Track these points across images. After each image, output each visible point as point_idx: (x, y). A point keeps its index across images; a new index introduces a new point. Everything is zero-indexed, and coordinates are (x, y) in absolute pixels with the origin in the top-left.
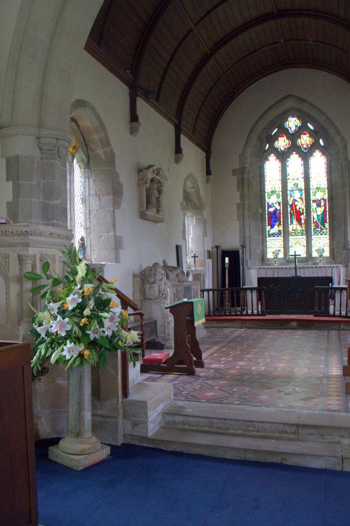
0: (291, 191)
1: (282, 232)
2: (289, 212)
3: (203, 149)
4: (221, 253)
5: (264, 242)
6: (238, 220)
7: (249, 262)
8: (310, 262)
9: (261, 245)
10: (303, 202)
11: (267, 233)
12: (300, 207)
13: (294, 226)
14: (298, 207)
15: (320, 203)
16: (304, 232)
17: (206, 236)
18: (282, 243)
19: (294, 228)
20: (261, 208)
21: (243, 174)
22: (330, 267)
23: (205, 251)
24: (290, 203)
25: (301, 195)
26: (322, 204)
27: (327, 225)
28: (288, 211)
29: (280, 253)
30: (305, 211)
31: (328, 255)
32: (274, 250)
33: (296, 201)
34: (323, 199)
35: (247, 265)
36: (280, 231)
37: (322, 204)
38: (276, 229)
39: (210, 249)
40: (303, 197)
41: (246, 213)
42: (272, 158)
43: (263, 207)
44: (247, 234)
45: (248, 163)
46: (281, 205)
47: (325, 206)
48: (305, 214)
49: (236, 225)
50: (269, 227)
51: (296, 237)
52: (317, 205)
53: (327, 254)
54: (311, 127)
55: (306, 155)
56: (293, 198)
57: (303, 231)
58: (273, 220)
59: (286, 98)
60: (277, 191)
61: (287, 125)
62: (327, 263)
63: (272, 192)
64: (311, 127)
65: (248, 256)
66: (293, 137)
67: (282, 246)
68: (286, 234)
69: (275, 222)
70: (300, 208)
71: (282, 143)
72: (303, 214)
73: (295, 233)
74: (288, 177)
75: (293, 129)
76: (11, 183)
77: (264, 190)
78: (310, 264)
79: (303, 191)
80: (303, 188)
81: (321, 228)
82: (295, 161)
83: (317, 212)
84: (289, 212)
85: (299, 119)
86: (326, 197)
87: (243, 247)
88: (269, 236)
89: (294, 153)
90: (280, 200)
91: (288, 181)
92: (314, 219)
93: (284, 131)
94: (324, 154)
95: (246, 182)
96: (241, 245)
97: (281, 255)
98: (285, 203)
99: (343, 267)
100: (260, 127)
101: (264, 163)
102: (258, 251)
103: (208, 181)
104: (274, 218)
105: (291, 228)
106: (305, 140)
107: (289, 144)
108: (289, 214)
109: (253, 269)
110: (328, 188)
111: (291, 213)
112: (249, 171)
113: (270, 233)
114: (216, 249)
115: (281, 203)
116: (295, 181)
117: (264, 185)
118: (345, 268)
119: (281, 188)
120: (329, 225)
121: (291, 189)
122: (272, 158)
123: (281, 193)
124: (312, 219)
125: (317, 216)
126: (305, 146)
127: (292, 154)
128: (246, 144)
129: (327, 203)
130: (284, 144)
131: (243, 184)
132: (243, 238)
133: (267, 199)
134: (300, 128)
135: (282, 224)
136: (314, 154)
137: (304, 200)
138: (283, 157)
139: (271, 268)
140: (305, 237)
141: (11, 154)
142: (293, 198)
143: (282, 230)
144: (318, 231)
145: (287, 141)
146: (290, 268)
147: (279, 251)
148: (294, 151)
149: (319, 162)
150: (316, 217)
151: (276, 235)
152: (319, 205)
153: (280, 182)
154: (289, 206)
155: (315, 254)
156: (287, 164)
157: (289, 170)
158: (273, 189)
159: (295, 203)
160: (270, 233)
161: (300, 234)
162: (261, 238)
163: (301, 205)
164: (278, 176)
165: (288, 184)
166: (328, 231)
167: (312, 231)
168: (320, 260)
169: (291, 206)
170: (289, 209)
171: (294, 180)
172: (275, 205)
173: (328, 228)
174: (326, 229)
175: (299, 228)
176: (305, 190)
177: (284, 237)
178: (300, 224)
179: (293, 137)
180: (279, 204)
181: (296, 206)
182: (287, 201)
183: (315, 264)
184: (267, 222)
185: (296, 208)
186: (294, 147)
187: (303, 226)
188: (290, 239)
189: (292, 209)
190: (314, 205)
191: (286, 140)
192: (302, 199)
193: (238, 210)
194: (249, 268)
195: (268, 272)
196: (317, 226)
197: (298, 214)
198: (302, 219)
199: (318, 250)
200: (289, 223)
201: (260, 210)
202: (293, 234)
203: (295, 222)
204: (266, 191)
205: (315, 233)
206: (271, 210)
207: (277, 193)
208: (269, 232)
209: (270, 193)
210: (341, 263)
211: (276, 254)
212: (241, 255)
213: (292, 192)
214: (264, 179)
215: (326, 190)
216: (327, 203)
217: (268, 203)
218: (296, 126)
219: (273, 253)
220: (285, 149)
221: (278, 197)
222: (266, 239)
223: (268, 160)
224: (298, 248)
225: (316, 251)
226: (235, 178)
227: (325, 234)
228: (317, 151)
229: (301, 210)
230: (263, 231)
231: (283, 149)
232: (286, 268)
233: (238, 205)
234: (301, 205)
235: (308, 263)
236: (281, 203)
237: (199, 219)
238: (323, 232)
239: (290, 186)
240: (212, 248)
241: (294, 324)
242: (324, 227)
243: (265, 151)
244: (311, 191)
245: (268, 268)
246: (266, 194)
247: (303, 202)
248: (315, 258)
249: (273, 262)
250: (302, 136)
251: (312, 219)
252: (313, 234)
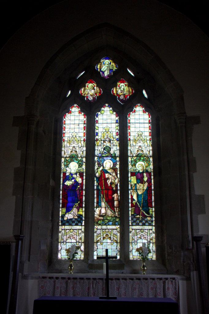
0: (99, 157)
1: (83, 219)
2: (95, 187)
6: (14, 194)
7: (26, 266)
8: (127, 269)
9: (49, 239)
10: (117, 175)
11: (60, 219)
13: (101, 210)
14: (109, 182)
15: (143, 177)
16: (117, 220)
22: (161, 279)
25: (115, 164)
26: (146, 179)
27: (152, 210)
28: (94, 186)
29: (79, 251)
30: (119, 188)
31: (154, 258)
32: (69, 246)
33: (108, 172)
34: (147, 172)
35: (22, 270)
36: (80, 216)
37: (146, 179)
40: (118, 166)
42: (75, 110)
44: (28, 217)
46: (84, 177)
47: (149, 181)
48: (119, 192)
50: (64, 210)
51: (104, 227)
52: (137, 179)
53: (152, 256)
55: (123, 110)
56: (101, 168)
57: (116, 217)
58: (70, 199)
60: (79, 156)
61: (98, 67)
62: (154, 272)
65: (25, 255)
66: (107, 84)
67: (83, 240)
68: (89, 222)
69: (74, 202)
70: (111, 183)
71: (90, 90)
72: (116, 192)
73: (103, 220)
75: (106, 74)
77: (61, 154)
78: (126, 273)
79: (118, 159)
80: (118, 153)
81: (143, 215)
83: (137, 191)
84: (95, 187)
85: (114, 62)
87: (18, 238)
88: (64, 224)
89: (107, 105)
91: (96, 142)
92: (133, 199)
96: (15, 236)
97: (80, 256)
98: (90, 174)
99: (182, 279)
101: (65, 116)
102: (44, 247)
104: (72, 196)
105: (97, 211)
106: (122, 89)
107: (100, 93)
108: (95, 192)
109: (32, 278)
110: (153, 156)
111: (98, 190)
113: (65, 219)
117: (61, 147)
118: (185, 282)
119: (85, 152)
120: (155, 211)
121: (100, 155)
122: (75, 110)
123: (84, 160)
124: (130, 201)
125: (138, 195)
126: (122, 97)
129: (152, 177)
132: (20, 224)
133: (63, 166)
134: (116, 73)
135: (84, 205)
138: (91, 110)
139: (63, 278)
142: (101, 168)
143: (84, 215)
144: (138, 219)
146: (94, 279)
147: (78, 248)
149: (140, 121)
150: (135, 197)
151: (74, 222)
152: (140, 180)
155: (134, 255)
158: (74, 153)
160: (65, 219)
161: (111, 223)
162: (51, 226)
163: (113, 179)
164: (81, 133)
166: (154, 219)
167: (130, 219)
168: (144, 266)
169: (99, 179)
170: (96, 183)
172: (75, 176)
173: (154, 215)
174: (151, 217)
175: (109, 212)
176: (120, 156)
179: (107, 84)
180: (81, 175)
181: (106, 179)
183: (135, 272)
184: (61, 201)
185: (106, 184)
186: (107, 98)
187: (117, 210)
188: (95, 230)
189: (100, 184)
190: (133, 180)
194: (25, 277)
195: (58, 285)
196: (137, 211)
197: (107, 192)
198: (116, 198)
199: (141, 248)
200: (95, 204)
201: (52, 183)
202: (99, 222)
205: (135, 222)
206: (68, 183)
207: (80, 159)
208: (63, 216)
209: (68, 159)
210: (177, 272)
211: (72, 252)
212: (13, 253)
213: (101, 159)
215: (151, 159)
216: (152, 177)
217: (65, 174)
218: (111, 70)
219: (68, 251)
220: (94, 98)
221: (80, 166)
222: (58, 229)
223: (70, 112)
224: (106, 246)
225: (138, 250)
227: (150, 225)
229: (113, 186)
231: (91, 98)
232: (88, 279)
234: (113, 179)
235: (124, 271)
238: (147, 221)
239: (98, 150)
242: (148, 213)
243: (65, 98)
244: (130, 159)
245: (57, 278)
246: (63, 160)
247: (117, 175)
248: (134, 261)
249: (67, 266)
250: (118, 83)
251: (130, 201)
252: (130, 224)
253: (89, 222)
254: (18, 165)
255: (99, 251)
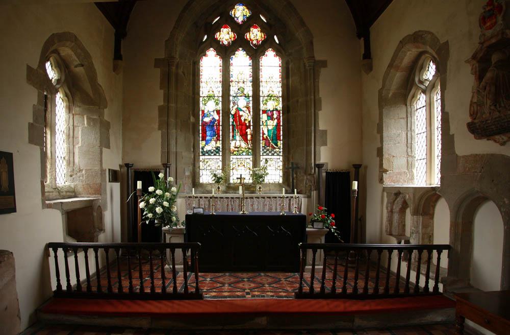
0: (234, 97)
2: (231, 123)
3: (114, 24)
4: (133, 174)
6: (159, 129)
10: (250, 112)
11: (201, 150)
12: (246, 118)
13: (237, 142)
14: (243, 119)
17: (108, 147)
18: (220, 164)
19: (238, 144)
20: (194, 116)
23: (103, 171)
24: (233, 112)
25: (248, 103)
28: (229, 122)
30: (251, 124)
36: (217, 148)
38: (212, 146)
39: (117, 168)
40: (251, 105)
41: (172, 120)
42: (211, 53)
43: (196, 116)
44: (173, 149)
45: (178, 53)
46: (221, 114)
48: (251, 127)
49: (157, 136)
55: (255, 53)
56: (236, 106)
60: (216, 95)
63: (209, 97)
66: (240, 29)
68: (225, 152)
70: (245, 120)
71: (225, 35)
72: (249, 127)
73: (238, 151)
74: (231, 79)
75: (240, 20)
79: (251, 98)
80: (251, 94)
82: (241, 61)
84: (231, 123)
85: (248, 8)
89: (241, 49)
90: (220, 107)
95: (173, 79)
98: (226, 112)
101: (201, 58)
105: (233, 144)
106: (255, 35)
109: (180, 197)
111: (233, 125)
112: (178, 63)
113: (205, 150)
114: (126, 168)
115: (221, 112)
116: (241, 85)
117: (199, 87)
121: (235, 95)
122: (211, 53)
126: (255, 42)
127: (237, 50)
130: (227, 37)
131: (168, 80)
133: (201, 105)
135: (221, 139)
136: (266, 53)
137: (251, 110)
138: (226, 53)
143: (221, 148)
145: (232, 34)
148: (240, 47)
149: (271, 63)
151: (212, 153)
153: (220, 85)
154: (231, 115)
156: (231, 62)
158: (211, 93)
159: (239, 114)
160: (205, 150)
163: (247, 116)
164: (218, 76)
165: (231, 88)
169: (234, 116)
170: (231, 120)
171: (238, 82)
172: (212, 113)
175: (243, 145)
177: (223, 156)
178: (246, 140)
179: (240, 29)
180: (218, 112)
182: (229, 109)
184: (201, 135)
186: (240, 42)
188: (231, 159)
191: (230, 33)
192: (248, 108)
193: (160, 116)
198: (248, 133)
201: (192, 119)
202: (235, 153)
203: (238, 137)
204: (201, 95)
207: (216, 98)
214: (199, 79)
217: (203, 111)
220: (229, 43)
221: (217, 104)
224: (241, 171)
226: (158, 71)
228: (270, 49)
229: (247, 122)
230: (195, 146)
233: (161, 109)
234: (247, 116)
236: (221, 112)
237: (94, 120)
239: (233, 90)
240: (121, 166)
244: (261, 99)
245: (201, 197)
247: (250, 112)
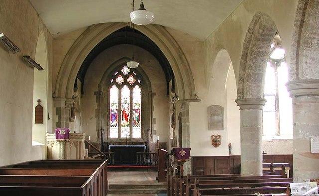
5: (108, 129)
13: (124, 122)
21: (100, 95)
27: (140, 122)
38: (114, 123)
40: (129, 107)
41: (100, 115)
42: (114, 86)
49: (95, 120)
54: (134, 73)
55: (131, 87)
59: (123, 58)
63: (113, 104)
64: (134, 73)
66: (125, 77)
68: (119, 126)
71: (120, 80)
76: (58, 116)
82: (125, 89)
83: (135, 116)
86: (140, 108)
93: (121, 74)
94: (140, 87)
95: (101, 99)
98: (120, 110)
100: (109, 71)
103: (82, 97)
106: (131, 79)
122: (114, 86)
128: (102, 79)
131: (99, 99)
138: (120, 86)
140: (129, 128)
141: (57, 107)
149: (137, 90)
152: (136, 112)
157: (122, 93)
163: (128, 112)
169: (123, 112)
175: (126, 123)
179: (125, 77)
180: (117, 110)
186: (125, 82)
190: (134, 112)
197: (126, 116)
203: (124, 120)
206: (113, 113)
221: (116, 107)
230: (108, 123)
239: (122, 102)
241: (128, 169)
244: (133, 105)
253: (119, 126)
254: (97, 108)
255: (123, 136)
